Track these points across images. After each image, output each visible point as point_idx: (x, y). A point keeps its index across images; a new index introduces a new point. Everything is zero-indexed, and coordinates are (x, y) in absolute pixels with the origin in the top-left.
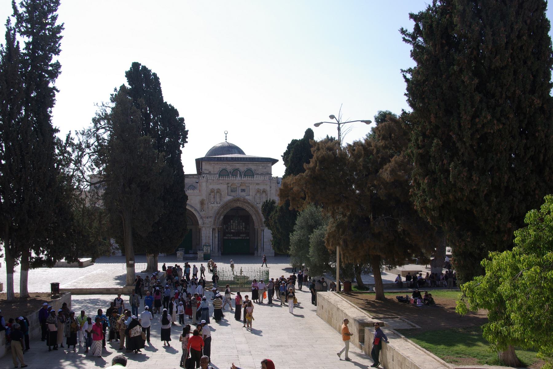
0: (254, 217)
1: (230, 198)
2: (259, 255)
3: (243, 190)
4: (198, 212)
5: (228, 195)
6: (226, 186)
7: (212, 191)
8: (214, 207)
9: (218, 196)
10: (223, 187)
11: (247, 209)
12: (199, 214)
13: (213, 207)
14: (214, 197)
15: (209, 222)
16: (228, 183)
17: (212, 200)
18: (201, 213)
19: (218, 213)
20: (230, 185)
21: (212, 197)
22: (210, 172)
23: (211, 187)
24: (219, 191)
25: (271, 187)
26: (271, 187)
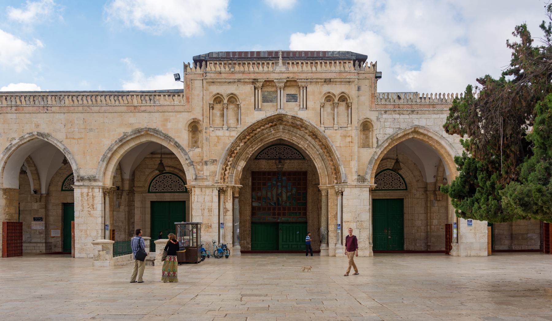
0: (318, 164)
1: (260, 116)
3: (292, 98)
4: (183, 150)
5: (256, 108)
6: (249, 88)
7: (218, 99)
8: (222, 136)
9: (230, 113)
11: (302, 145)
12: (186, 154)
13: (218, 137)
14: (223, 115)
15: (212, 172)
16: (254, 81)
17: (218, 120)
18: (191, 154)
19: (231, 153)
20: (259, 85)
21: (217, 112)
23: (215, 89)
24: (233, 98)
25: (359, 89)
26: (359, 89)
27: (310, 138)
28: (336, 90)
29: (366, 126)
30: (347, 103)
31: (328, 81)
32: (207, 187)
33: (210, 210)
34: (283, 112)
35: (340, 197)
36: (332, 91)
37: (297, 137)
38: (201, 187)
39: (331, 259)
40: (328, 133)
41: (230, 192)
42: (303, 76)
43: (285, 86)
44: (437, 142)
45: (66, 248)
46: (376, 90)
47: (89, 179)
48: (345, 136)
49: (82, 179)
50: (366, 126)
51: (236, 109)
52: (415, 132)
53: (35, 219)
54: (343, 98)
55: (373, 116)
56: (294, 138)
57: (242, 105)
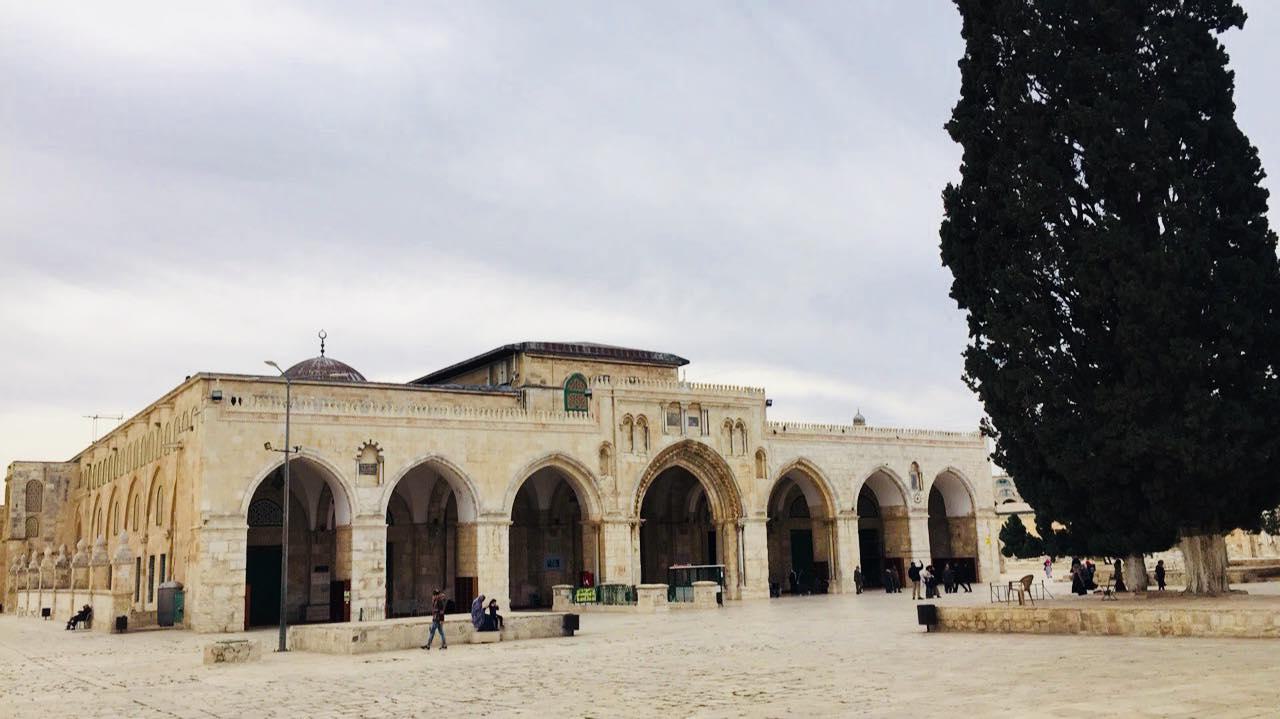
0: (712, 495)
2: (734, 596)
7: (628, 419)
10: (656, 417)
13: (629, 464)
17: (627, 444)
22: (543, 382)
23: (623, 409)
27: (708, 467)
28: (735, 416)
29: (760, 455)
30: (742, 430)
31: (727, 407)
32: (620, 523)
33: (624, 551)
34: (689, 437)
35: (740, 533)
36: (730, 416)
37: (694, 464)
38: (613, 523)
39: (733, 603)
40: (730, 461)
41: (637, 528)
42: (706, 399)
43: (690, 409)
44: (815, 472)
45: (339, 612)
46: (765, 417)
47: (496, 515)
48: (743, 466)
49: (488, 514)
50: (760, 455)
51: (643, 431)
52: (799, 463)
53: (318, 569)
54: (740, 426)
55: (765, 445)
56: (691, 466)
57: (651, 427)
